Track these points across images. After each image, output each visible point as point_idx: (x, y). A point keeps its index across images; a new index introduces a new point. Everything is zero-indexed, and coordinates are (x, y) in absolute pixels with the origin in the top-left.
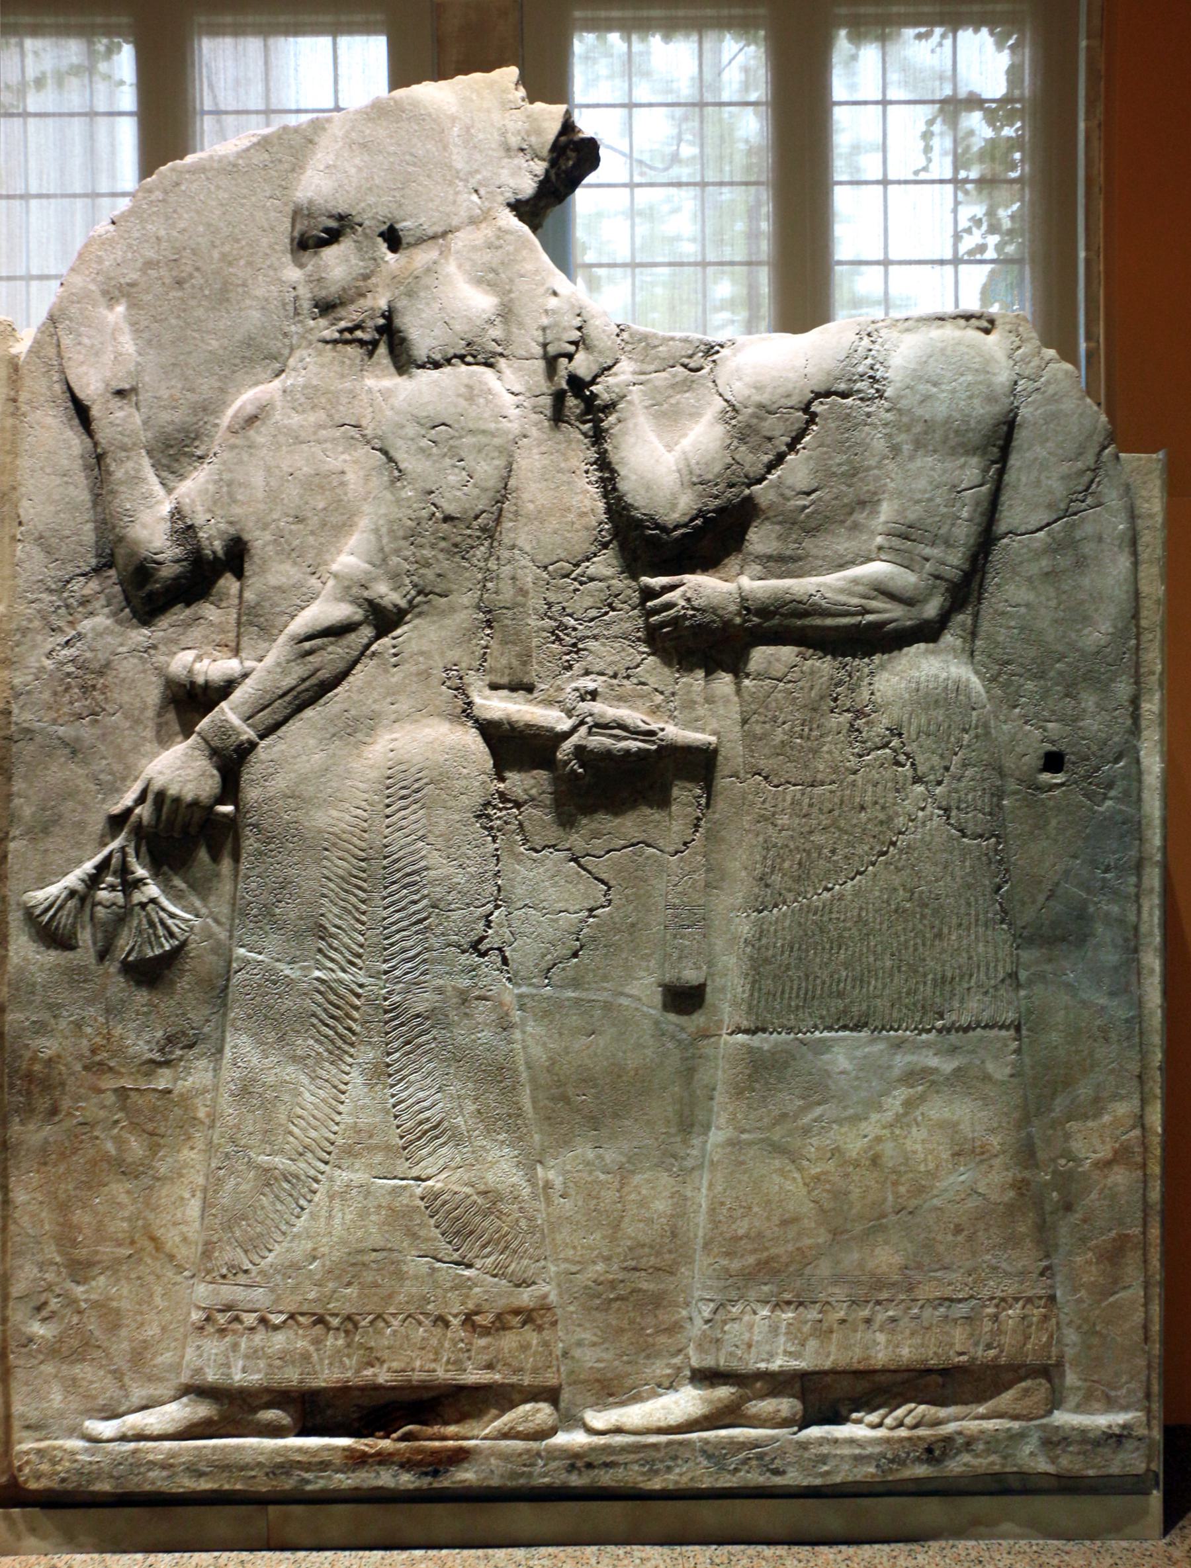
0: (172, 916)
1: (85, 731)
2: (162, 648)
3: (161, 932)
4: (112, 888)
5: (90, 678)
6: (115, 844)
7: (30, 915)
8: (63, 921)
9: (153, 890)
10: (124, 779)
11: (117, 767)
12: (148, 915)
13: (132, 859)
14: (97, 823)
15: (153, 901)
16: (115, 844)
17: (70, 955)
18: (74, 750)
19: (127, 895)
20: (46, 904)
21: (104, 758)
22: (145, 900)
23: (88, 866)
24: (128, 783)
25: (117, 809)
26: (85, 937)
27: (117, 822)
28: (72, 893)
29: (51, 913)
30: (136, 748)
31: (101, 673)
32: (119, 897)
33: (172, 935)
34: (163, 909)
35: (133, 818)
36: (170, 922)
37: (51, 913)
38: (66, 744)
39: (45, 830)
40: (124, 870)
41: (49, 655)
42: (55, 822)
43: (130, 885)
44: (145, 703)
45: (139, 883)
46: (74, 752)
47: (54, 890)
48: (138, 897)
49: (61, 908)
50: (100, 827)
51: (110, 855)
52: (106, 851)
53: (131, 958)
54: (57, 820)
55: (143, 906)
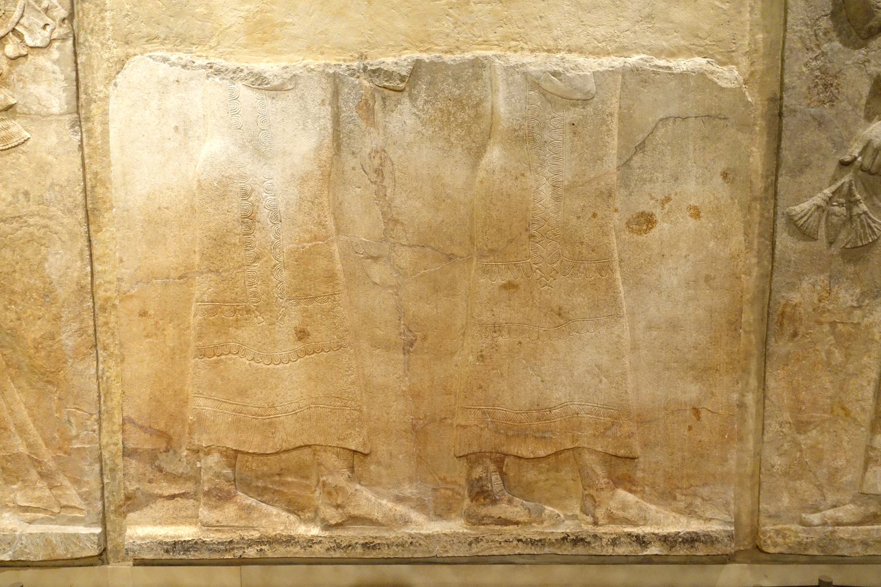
0: (874, 222)
1: (827, 111)
2: (873, 62)
3: (868, 231)
4: (840, 205)
5: (830, 80)
6: (846, 179)
7: (791, 220)
8: (812, 223)
9: (863, 207)
10: (849, 141)
11: (845, 134)
12: (862, 220)
13: (854, 188)
14: (832, 167)
15: (865, 213)
16: (846, 179)
17: (812, 243)
18: (821, 122)
19: (849, 209)
20: (802, 214)
21: (837, 127)
22: (860, 212)
23: (828, 192)
24: (851, 143)
25: (848, 158)
26: (822, 233)
27: (844, 164)
28: (819, 207)
29: (805, 219)
30: (856, 121)
31: (836, 77)
32: (843, 210)
33: (874, 232)
34: (870, 218)
35: (856, 163)
36: (873, 225)
37: (805, 219)
38: (814, 119)
39: (801, 171)
40: (850, 193)
41: (806, 65)
42: (807, 166)
43: (851, 203)
44: (861, 95)
45: (856, 202)
46: (820, 124)
47: (806, 205)
48: (856, 210)
49: (811, 216)
50: (834, 169)
51: (843, 184)
52: (839, 184)
53: (848, 246)
54: (808, 165)
55: (859, 215)
